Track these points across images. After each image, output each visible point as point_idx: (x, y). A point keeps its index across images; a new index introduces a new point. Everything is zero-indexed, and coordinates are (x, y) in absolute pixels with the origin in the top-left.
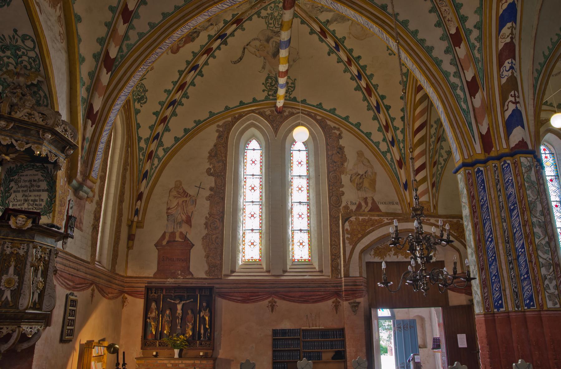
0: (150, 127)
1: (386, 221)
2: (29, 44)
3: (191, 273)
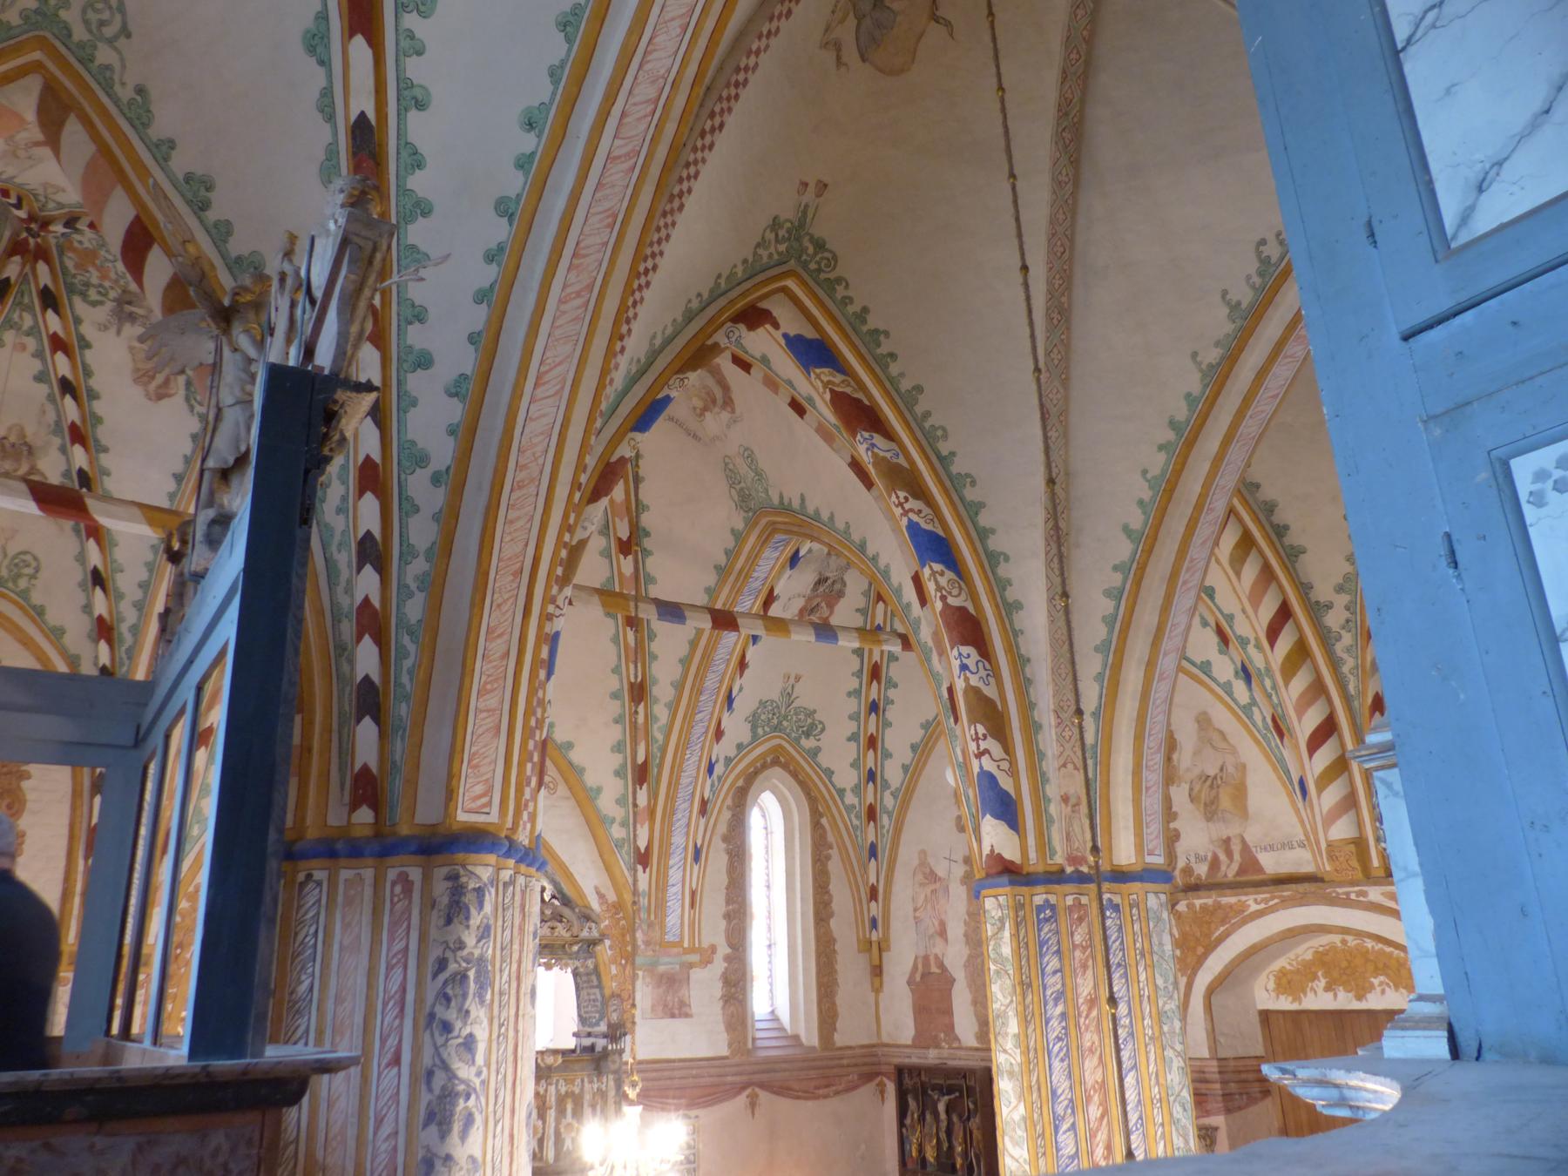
0: (852, 765)
1: (1254, 907)
3: (957, 1039)
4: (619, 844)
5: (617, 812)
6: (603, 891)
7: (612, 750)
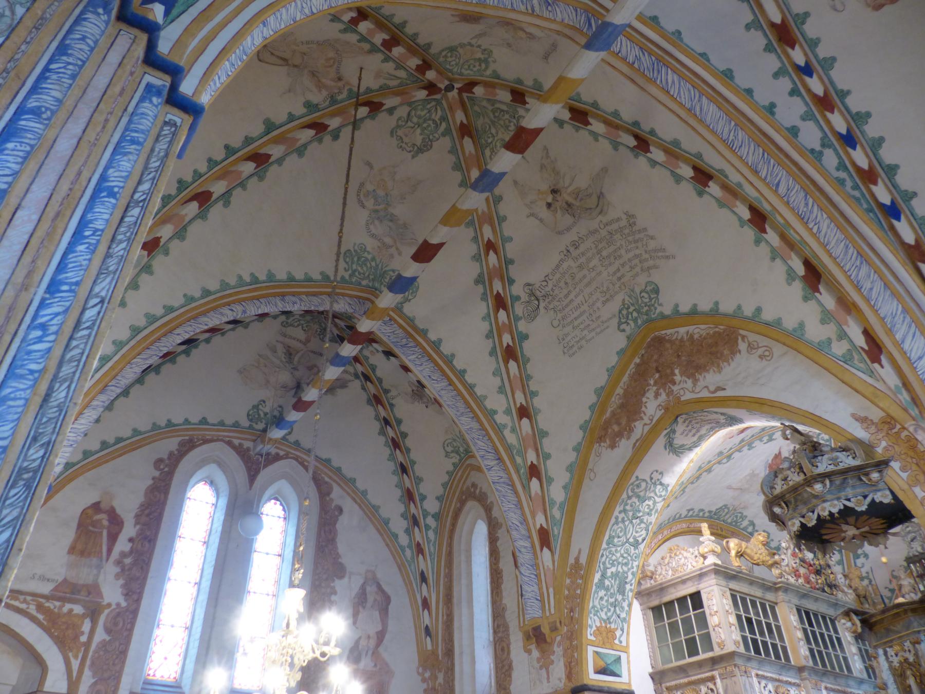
4: (847, 359)
5: (830, 331)
6: (863, 414)
7: (789, 284)
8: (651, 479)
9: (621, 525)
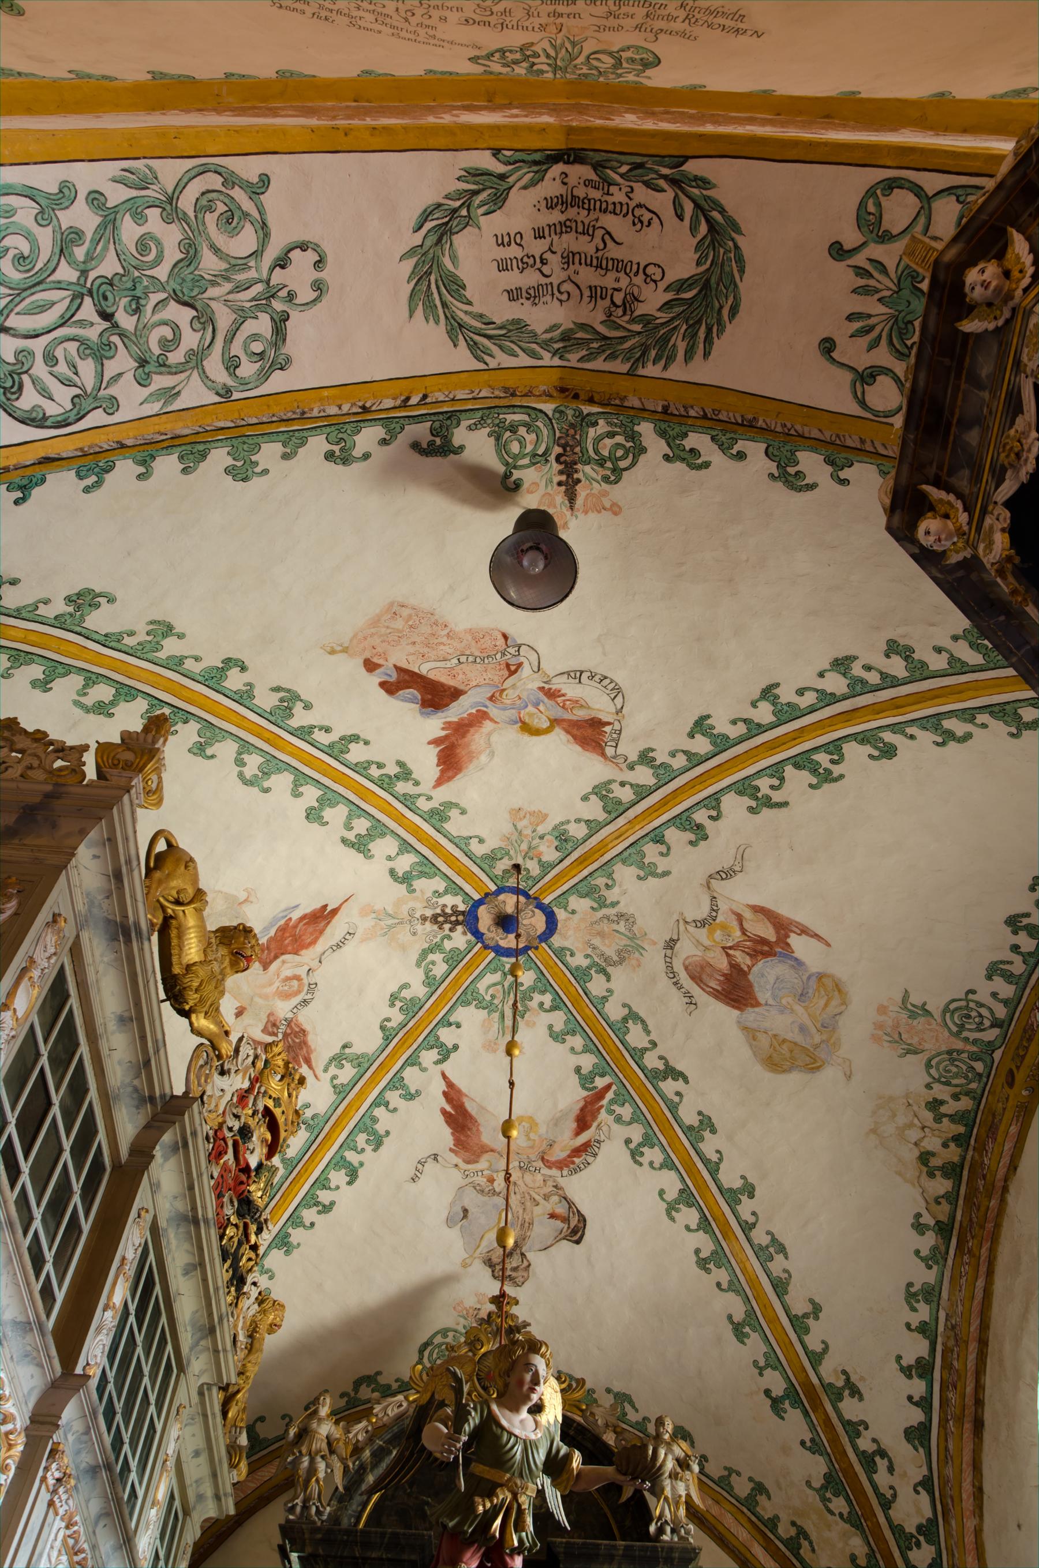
2: (899, 210)
8: (282, 263)
9: (45, 237)
